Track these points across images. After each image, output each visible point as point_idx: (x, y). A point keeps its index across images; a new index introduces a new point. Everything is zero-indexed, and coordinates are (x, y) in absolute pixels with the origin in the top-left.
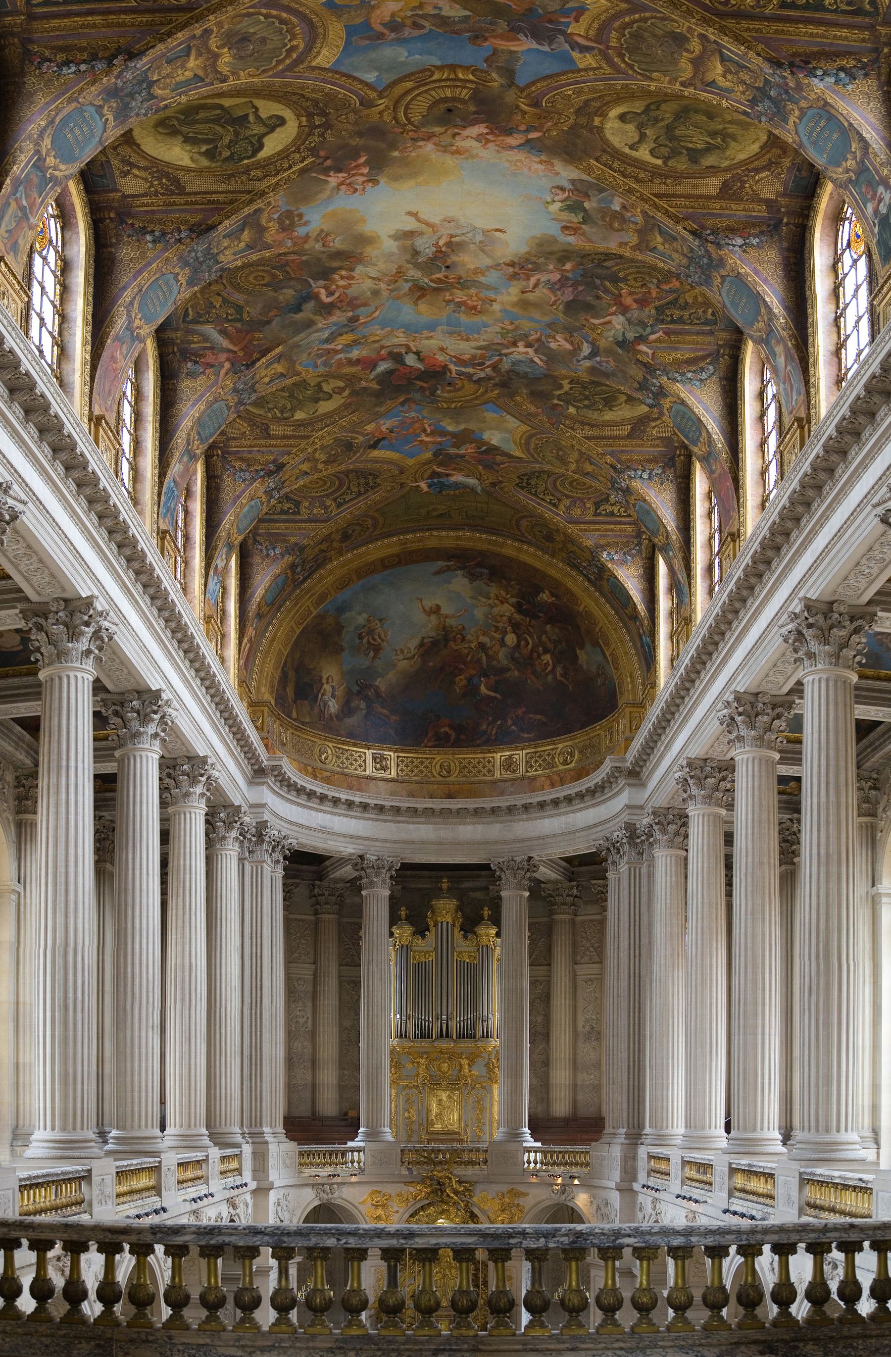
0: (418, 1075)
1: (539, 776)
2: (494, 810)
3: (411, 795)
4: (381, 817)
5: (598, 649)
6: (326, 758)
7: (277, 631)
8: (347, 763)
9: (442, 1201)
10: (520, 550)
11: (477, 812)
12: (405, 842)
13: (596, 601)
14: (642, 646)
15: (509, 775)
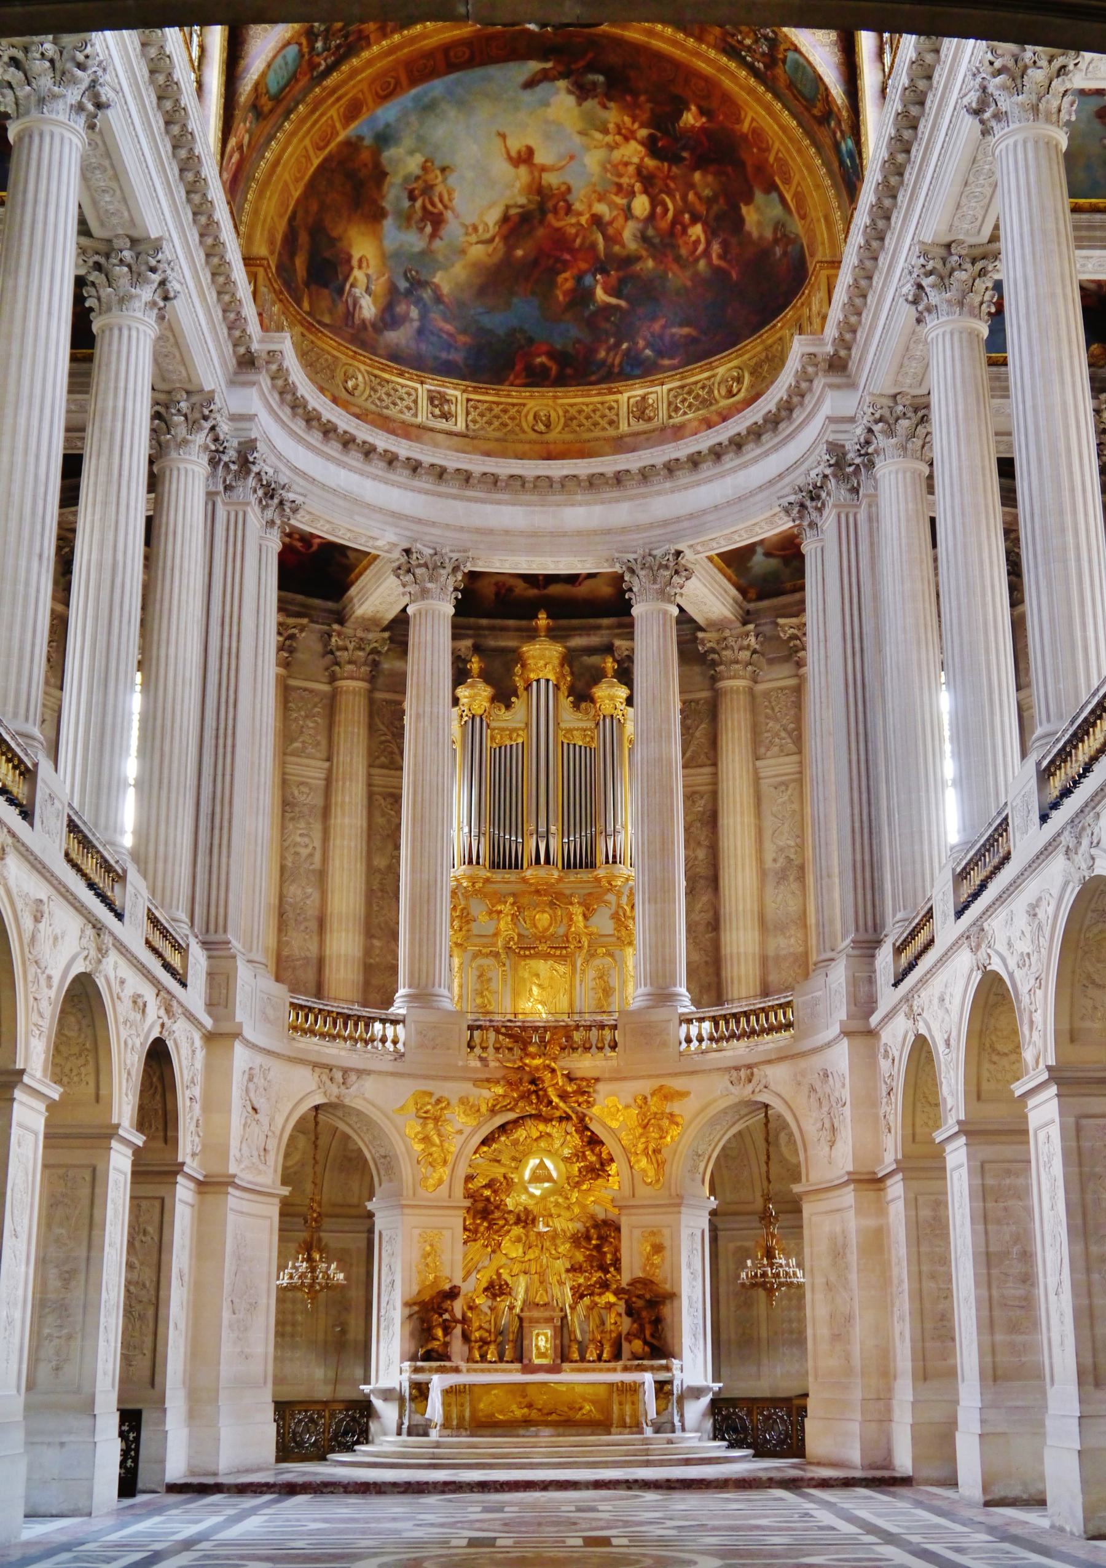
0: (496, 935)
1: (690, 420)
2: (619, 479)
3: (488, 454)
4: (442, 489)
5: (774, 195)
6: (356, 387)
7: (283, 150)
8: (387, 401)
9: (538, 1117)
10: (651, 33)
11: (593, 483)
12: (478, 531)
13: (768, 109)
14: (842, 163)
15: (642, 426)
